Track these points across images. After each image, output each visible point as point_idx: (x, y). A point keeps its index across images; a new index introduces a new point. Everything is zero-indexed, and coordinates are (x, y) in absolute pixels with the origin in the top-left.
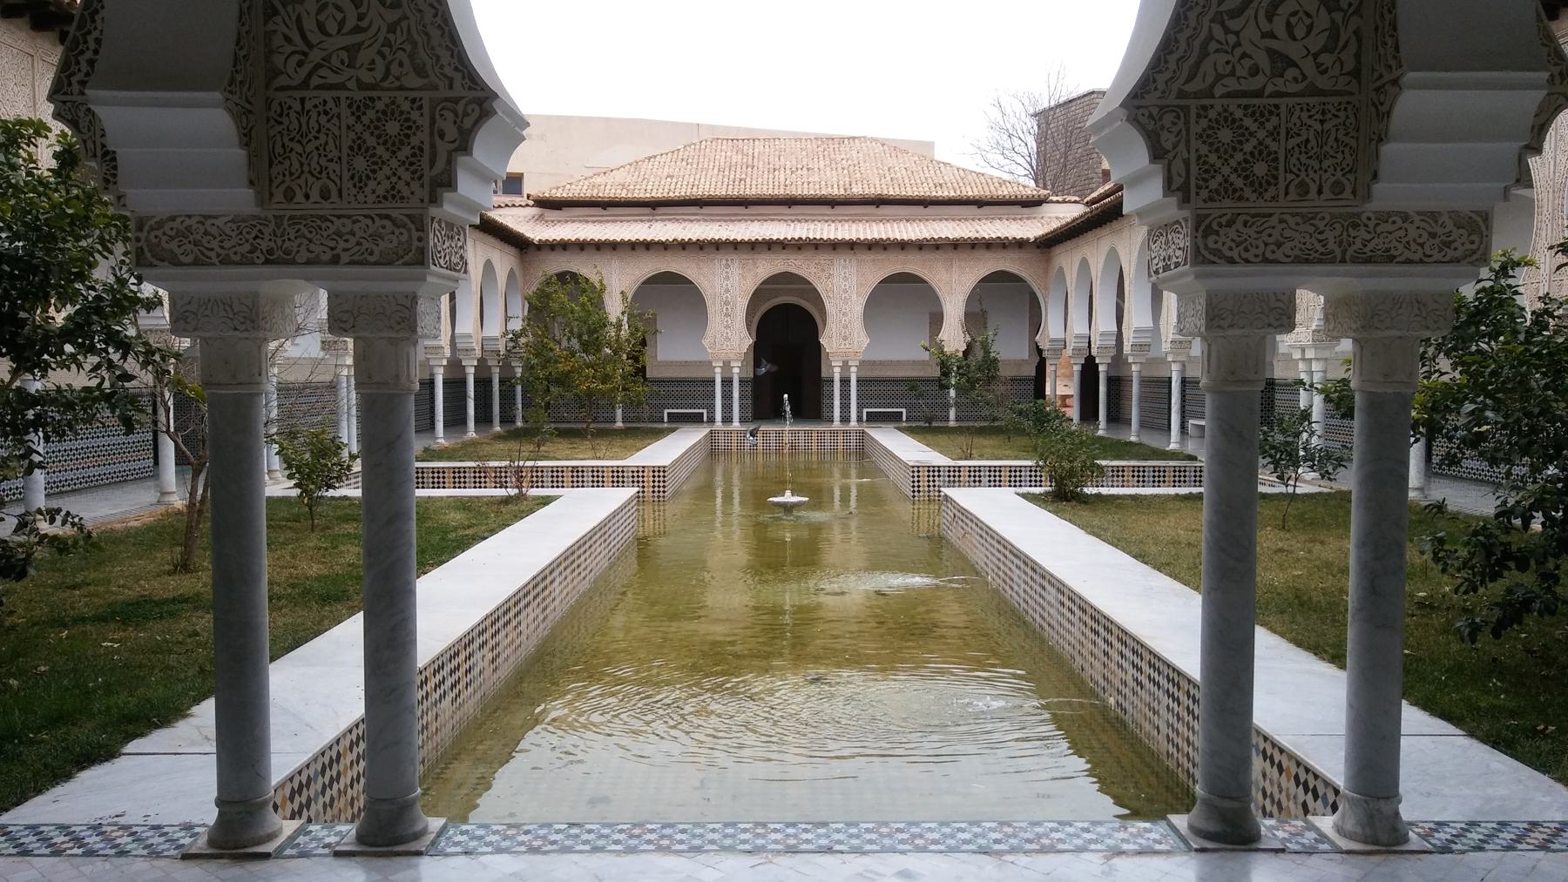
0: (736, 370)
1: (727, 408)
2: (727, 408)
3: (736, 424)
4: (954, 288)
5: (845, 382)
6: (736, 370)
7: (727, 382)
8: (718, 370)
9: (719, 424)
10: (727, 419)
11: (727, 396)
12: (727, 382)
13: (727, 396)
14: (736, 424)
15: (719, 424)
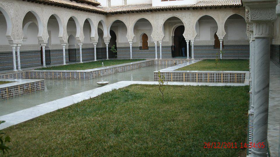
0: (160, 44)
1: (159, 54)
2: (159, 54)
3: (161, 58)
4: (221, 19)
5: (190, 47)
6: (160, 44)
7: (158, 47)
8: (156, 44)
9: (156, 59)
10: (159, 57)
11: (158, 51)
12: (158, 47)
13: (158, 51)
14: (161, 58)
15: (156, 59)
